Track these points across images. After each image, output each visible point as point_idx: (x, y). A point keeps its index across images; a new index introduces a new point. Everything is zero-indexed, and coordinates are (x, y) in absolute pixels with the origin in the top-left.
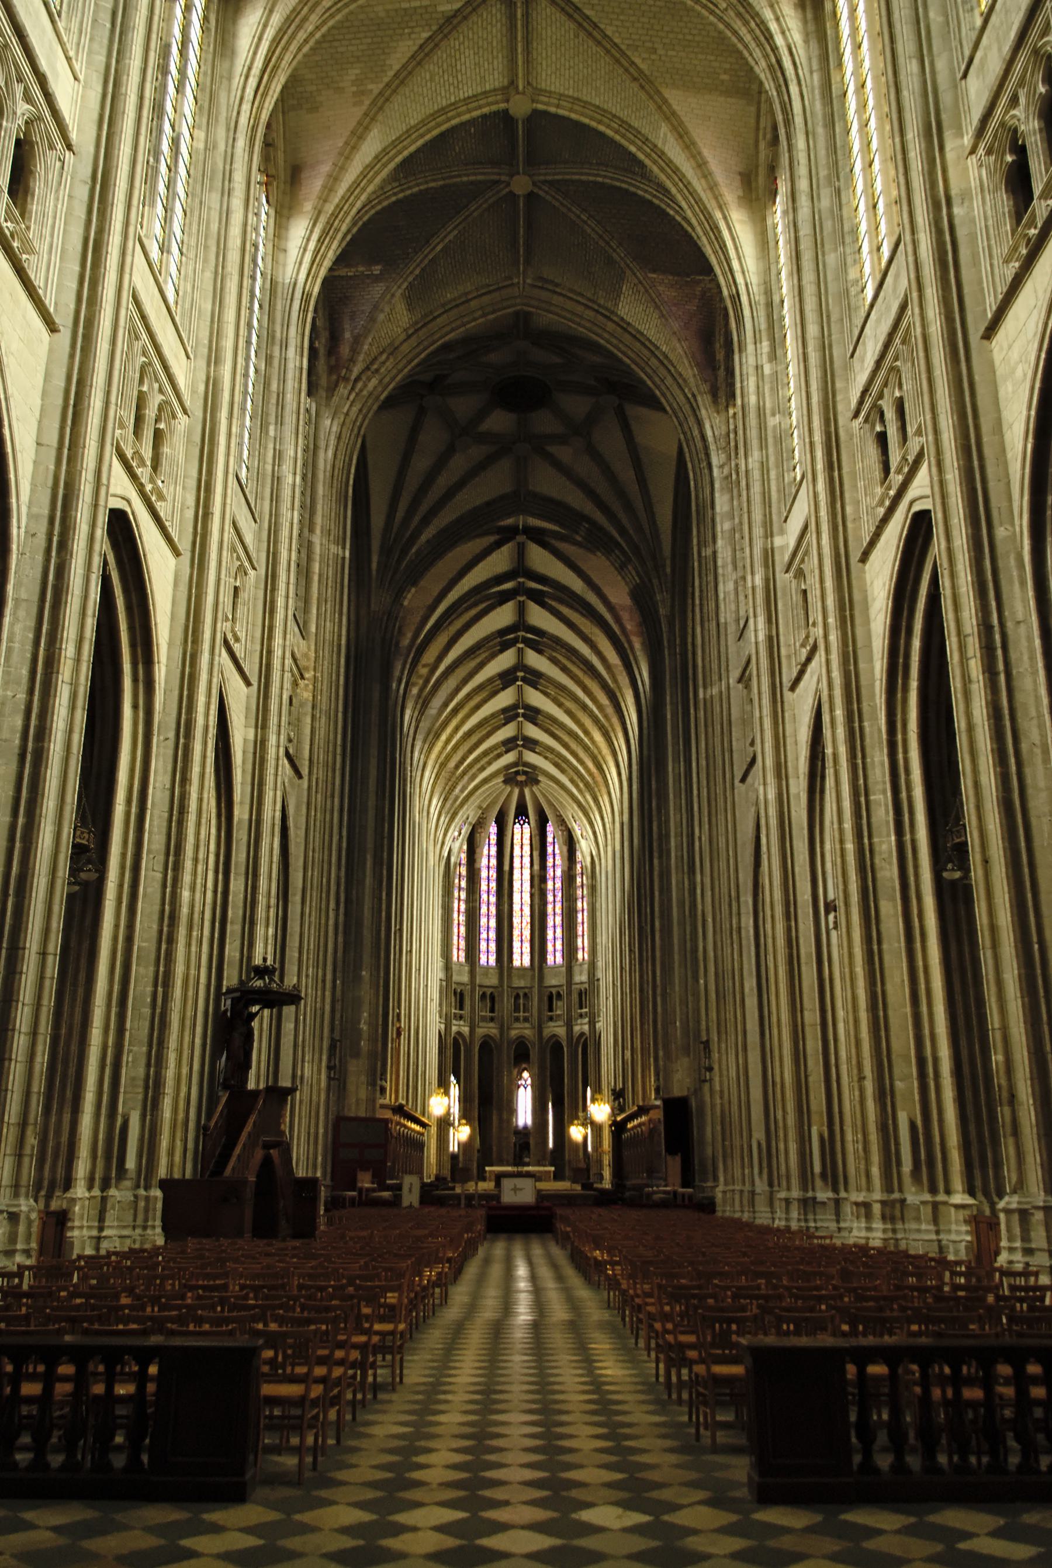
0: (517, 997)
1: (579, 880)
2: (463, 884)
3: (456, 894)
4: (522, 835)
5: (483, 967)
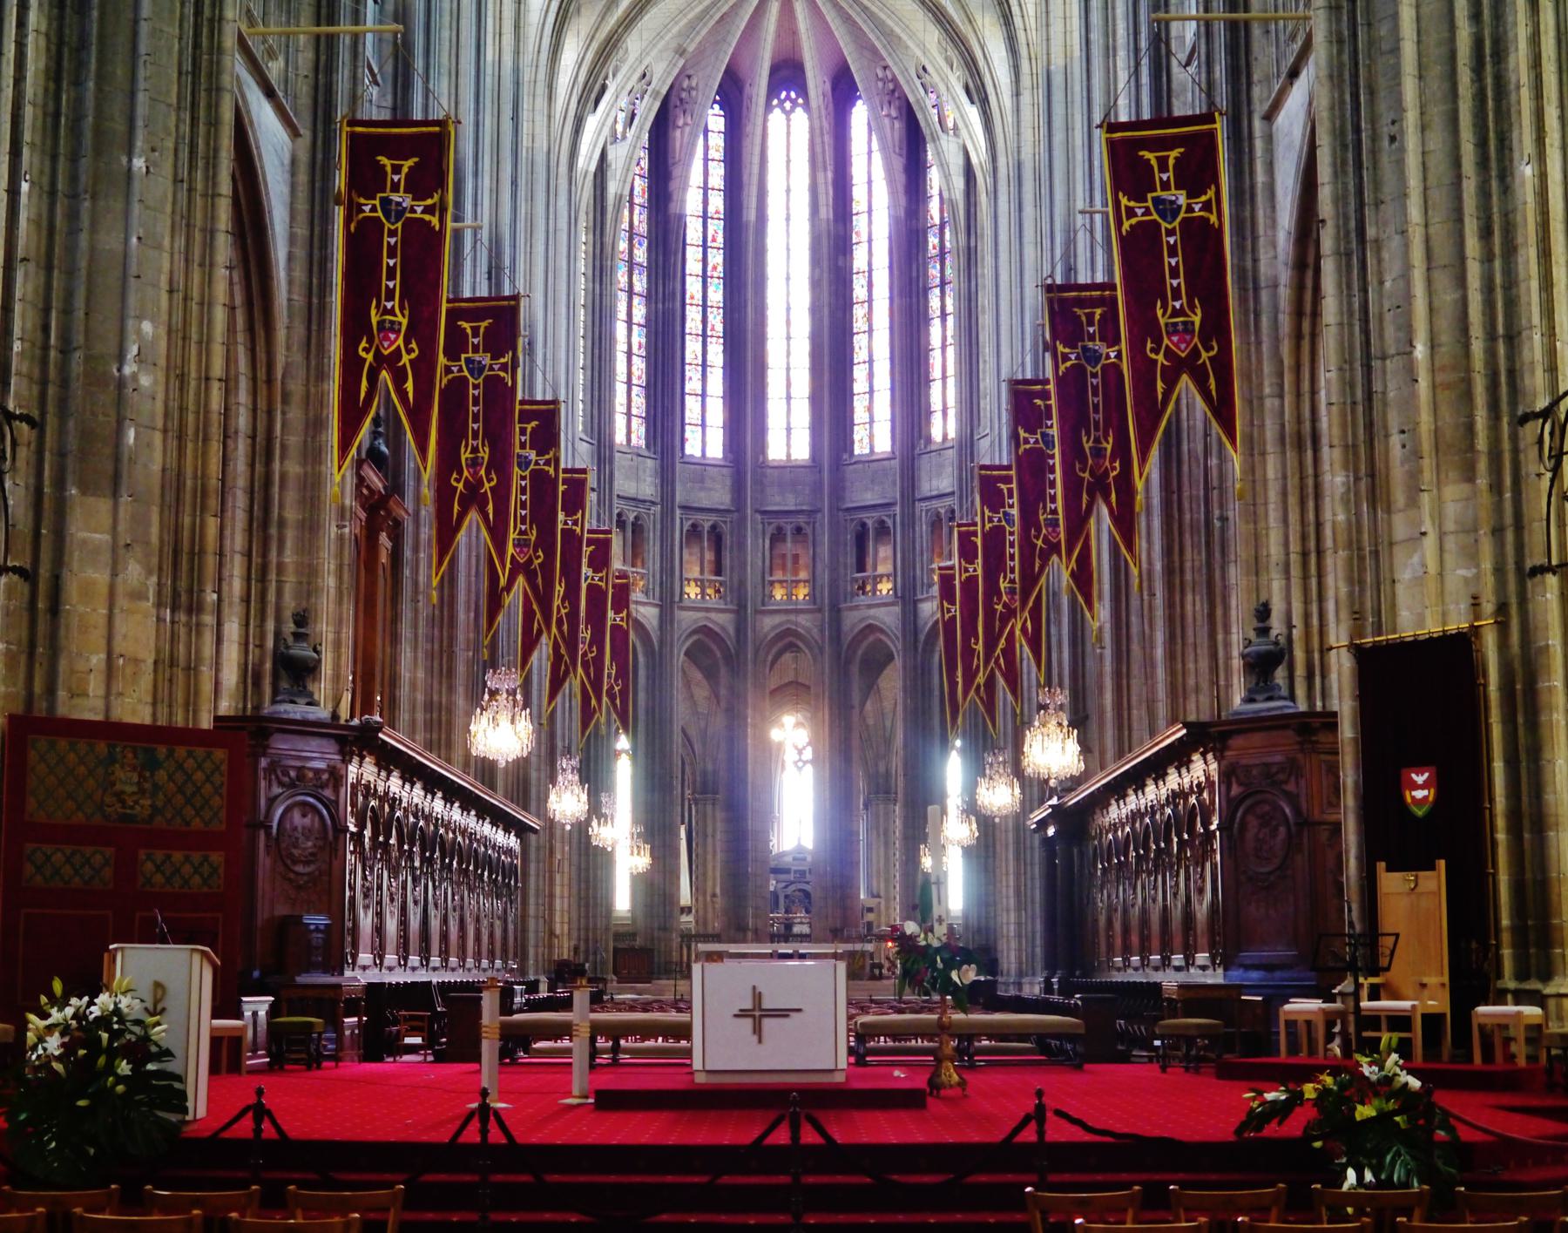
0: (778, 537)
1: (933, 240)
2: (641, 255)
3: (622, 278)
4: (787, 135)
5: (689, 462)
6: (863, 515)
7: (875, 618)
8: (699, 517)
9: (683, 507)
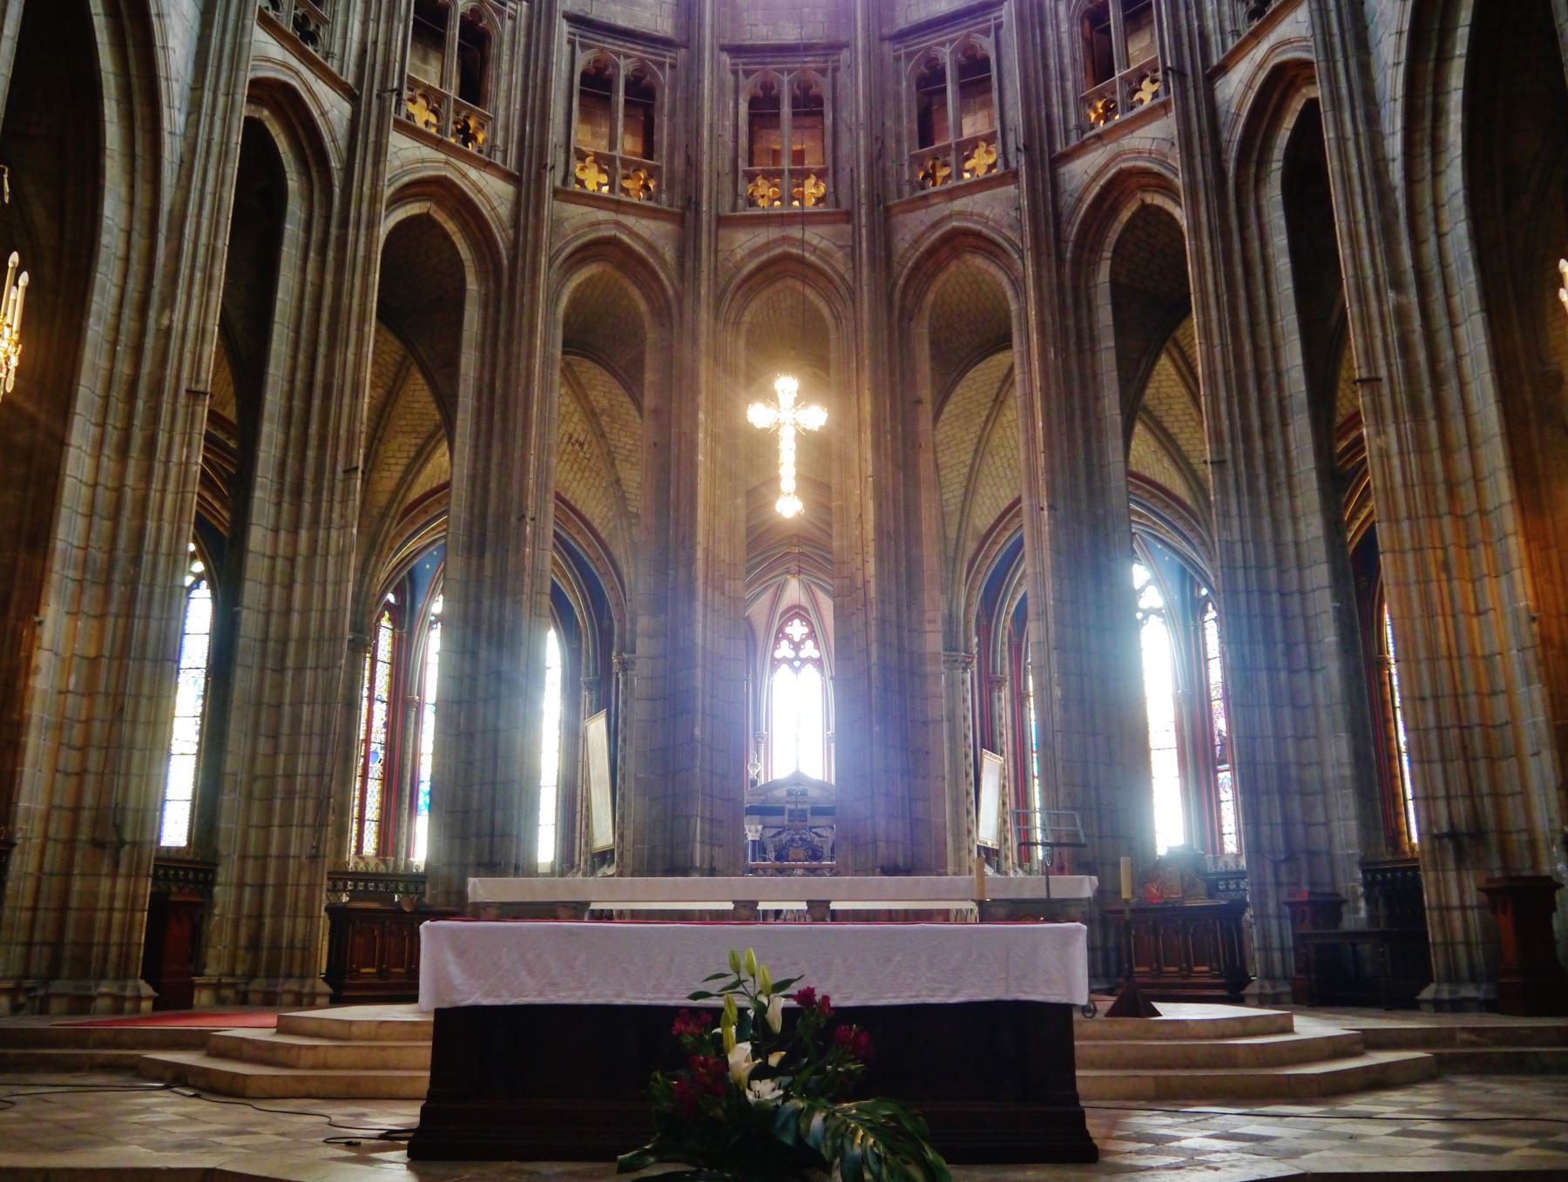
6: (930, 41)
7: (962, 214)
8: (611, 45)
9: (575, 20)
